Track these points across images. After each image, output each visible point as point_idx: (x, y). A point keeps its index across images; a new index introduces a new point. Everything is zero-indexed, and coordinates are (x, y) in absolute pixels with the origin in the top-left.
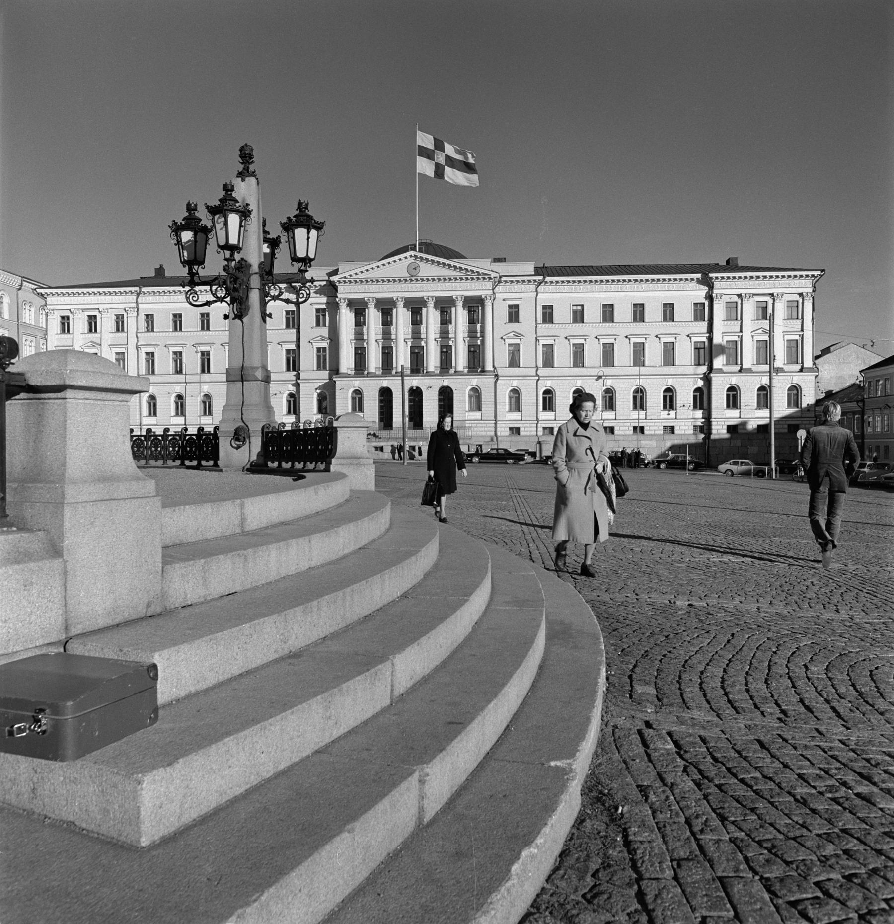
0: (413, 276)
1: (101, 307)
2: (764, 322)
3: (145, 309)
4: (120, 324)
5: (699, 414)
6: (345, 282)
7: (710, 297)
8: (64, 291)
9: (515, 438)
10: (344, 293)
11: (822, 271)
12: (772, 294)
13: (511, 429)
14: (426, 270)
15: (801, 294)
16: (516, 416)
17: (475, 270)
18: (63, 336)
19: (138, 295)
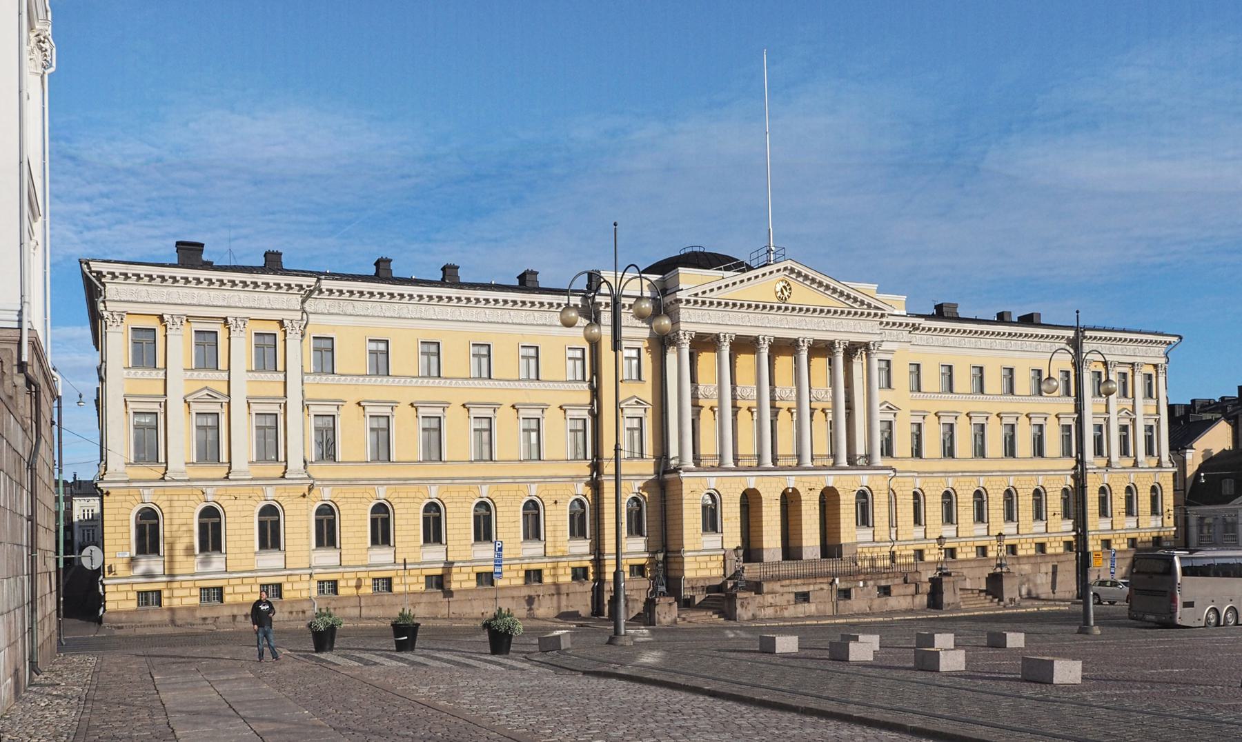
0: (782, 306)
1: (166, 311)
2: (1067, 398)
3: (320, 325)
4: (267, 352)
5: (583, 546)
6: (696, 302)
7: (1078, 364)
8: (143, 270)
9: (387, 598)
10: (692, 321)
11: (1181, 338)
12: (1133, 364)
13: (479, 575)
14: (802, 295)
15: (1156, 366)
16: (535, 548)
17: (860, 297)
18: (139, 373)
19: (308, 294)
